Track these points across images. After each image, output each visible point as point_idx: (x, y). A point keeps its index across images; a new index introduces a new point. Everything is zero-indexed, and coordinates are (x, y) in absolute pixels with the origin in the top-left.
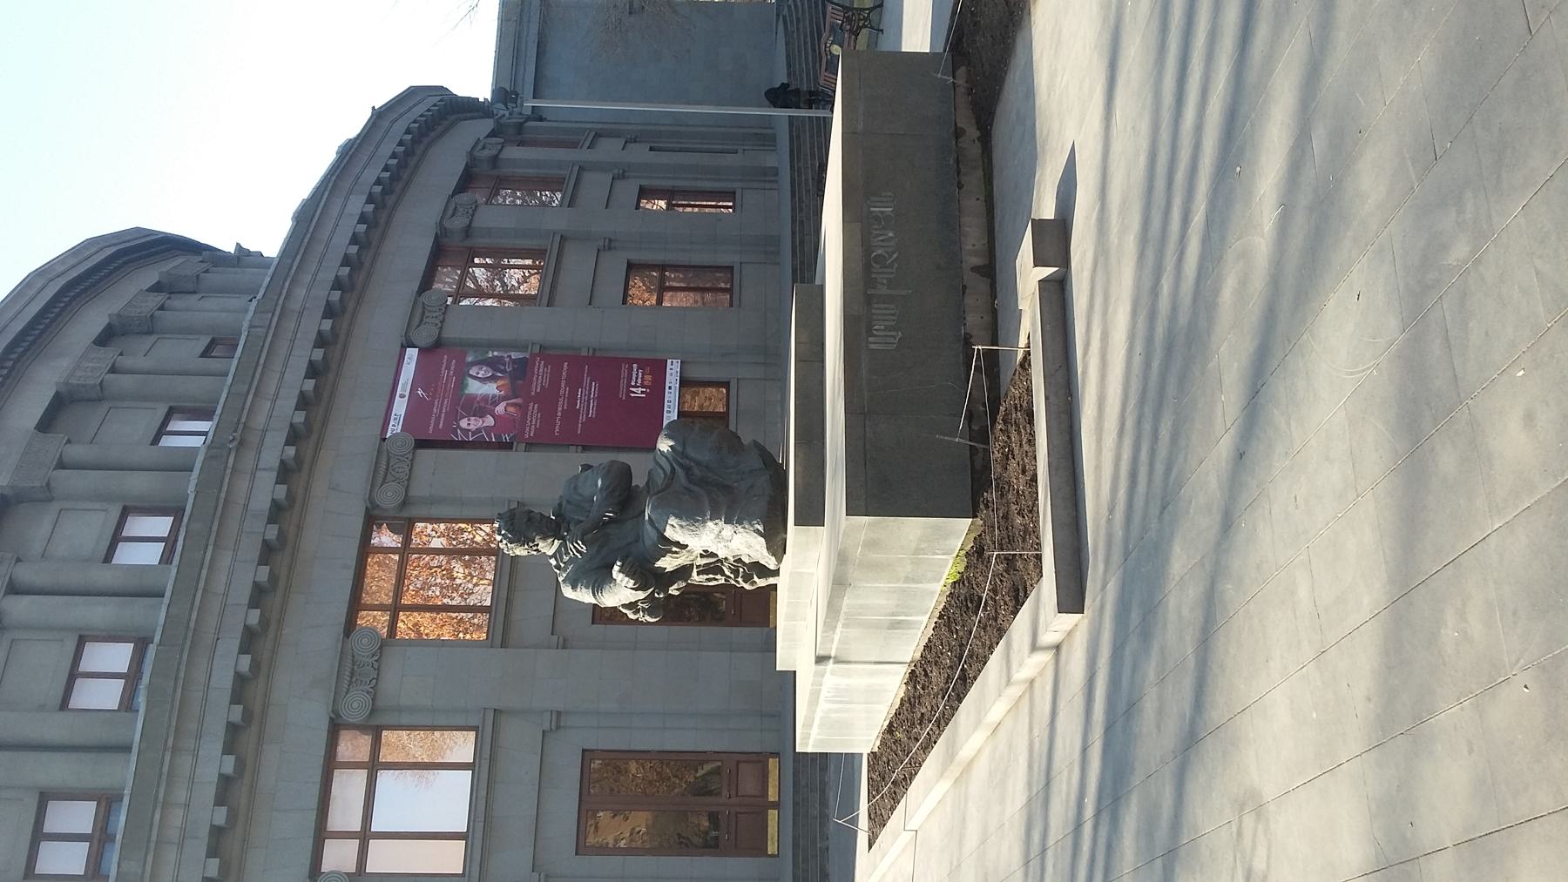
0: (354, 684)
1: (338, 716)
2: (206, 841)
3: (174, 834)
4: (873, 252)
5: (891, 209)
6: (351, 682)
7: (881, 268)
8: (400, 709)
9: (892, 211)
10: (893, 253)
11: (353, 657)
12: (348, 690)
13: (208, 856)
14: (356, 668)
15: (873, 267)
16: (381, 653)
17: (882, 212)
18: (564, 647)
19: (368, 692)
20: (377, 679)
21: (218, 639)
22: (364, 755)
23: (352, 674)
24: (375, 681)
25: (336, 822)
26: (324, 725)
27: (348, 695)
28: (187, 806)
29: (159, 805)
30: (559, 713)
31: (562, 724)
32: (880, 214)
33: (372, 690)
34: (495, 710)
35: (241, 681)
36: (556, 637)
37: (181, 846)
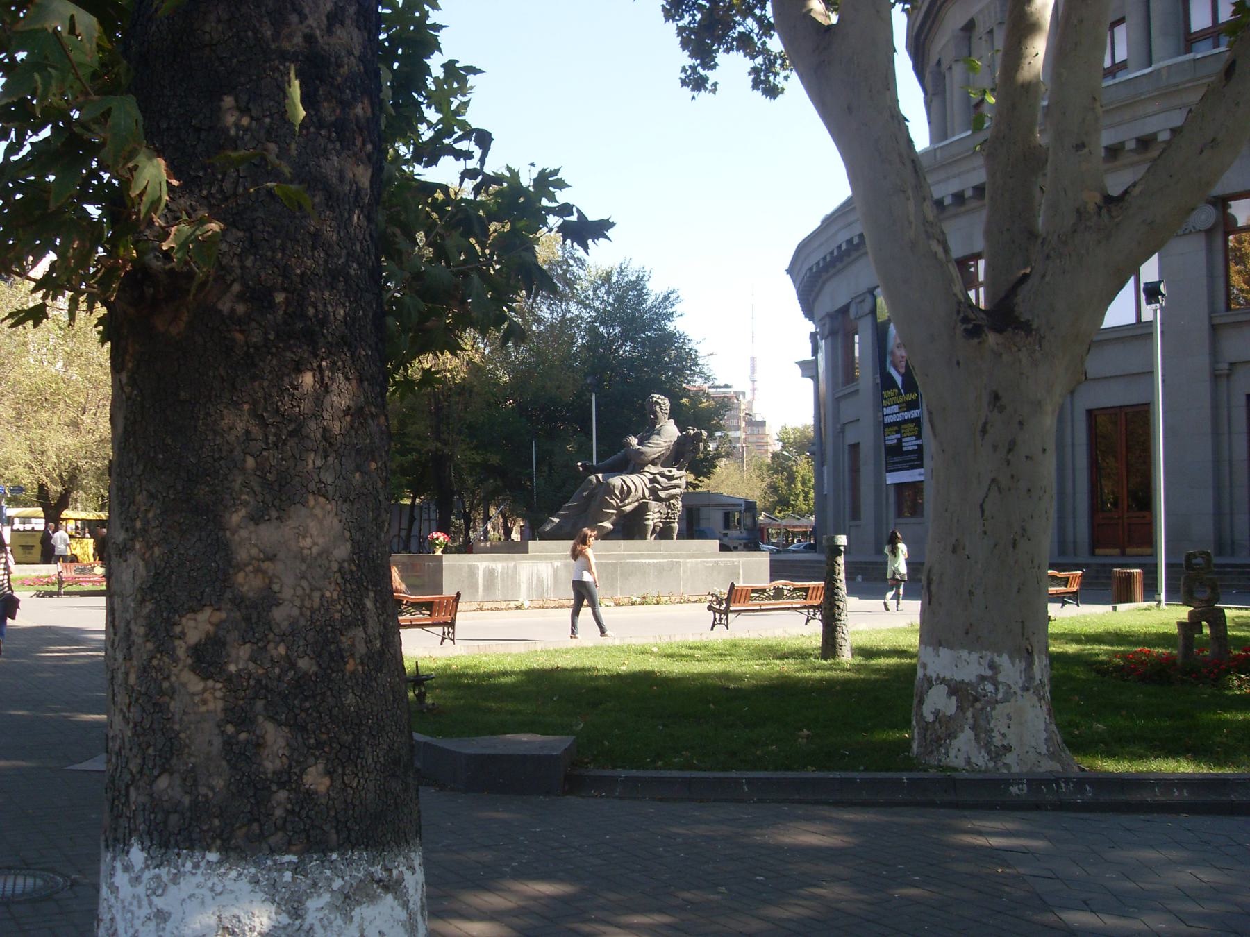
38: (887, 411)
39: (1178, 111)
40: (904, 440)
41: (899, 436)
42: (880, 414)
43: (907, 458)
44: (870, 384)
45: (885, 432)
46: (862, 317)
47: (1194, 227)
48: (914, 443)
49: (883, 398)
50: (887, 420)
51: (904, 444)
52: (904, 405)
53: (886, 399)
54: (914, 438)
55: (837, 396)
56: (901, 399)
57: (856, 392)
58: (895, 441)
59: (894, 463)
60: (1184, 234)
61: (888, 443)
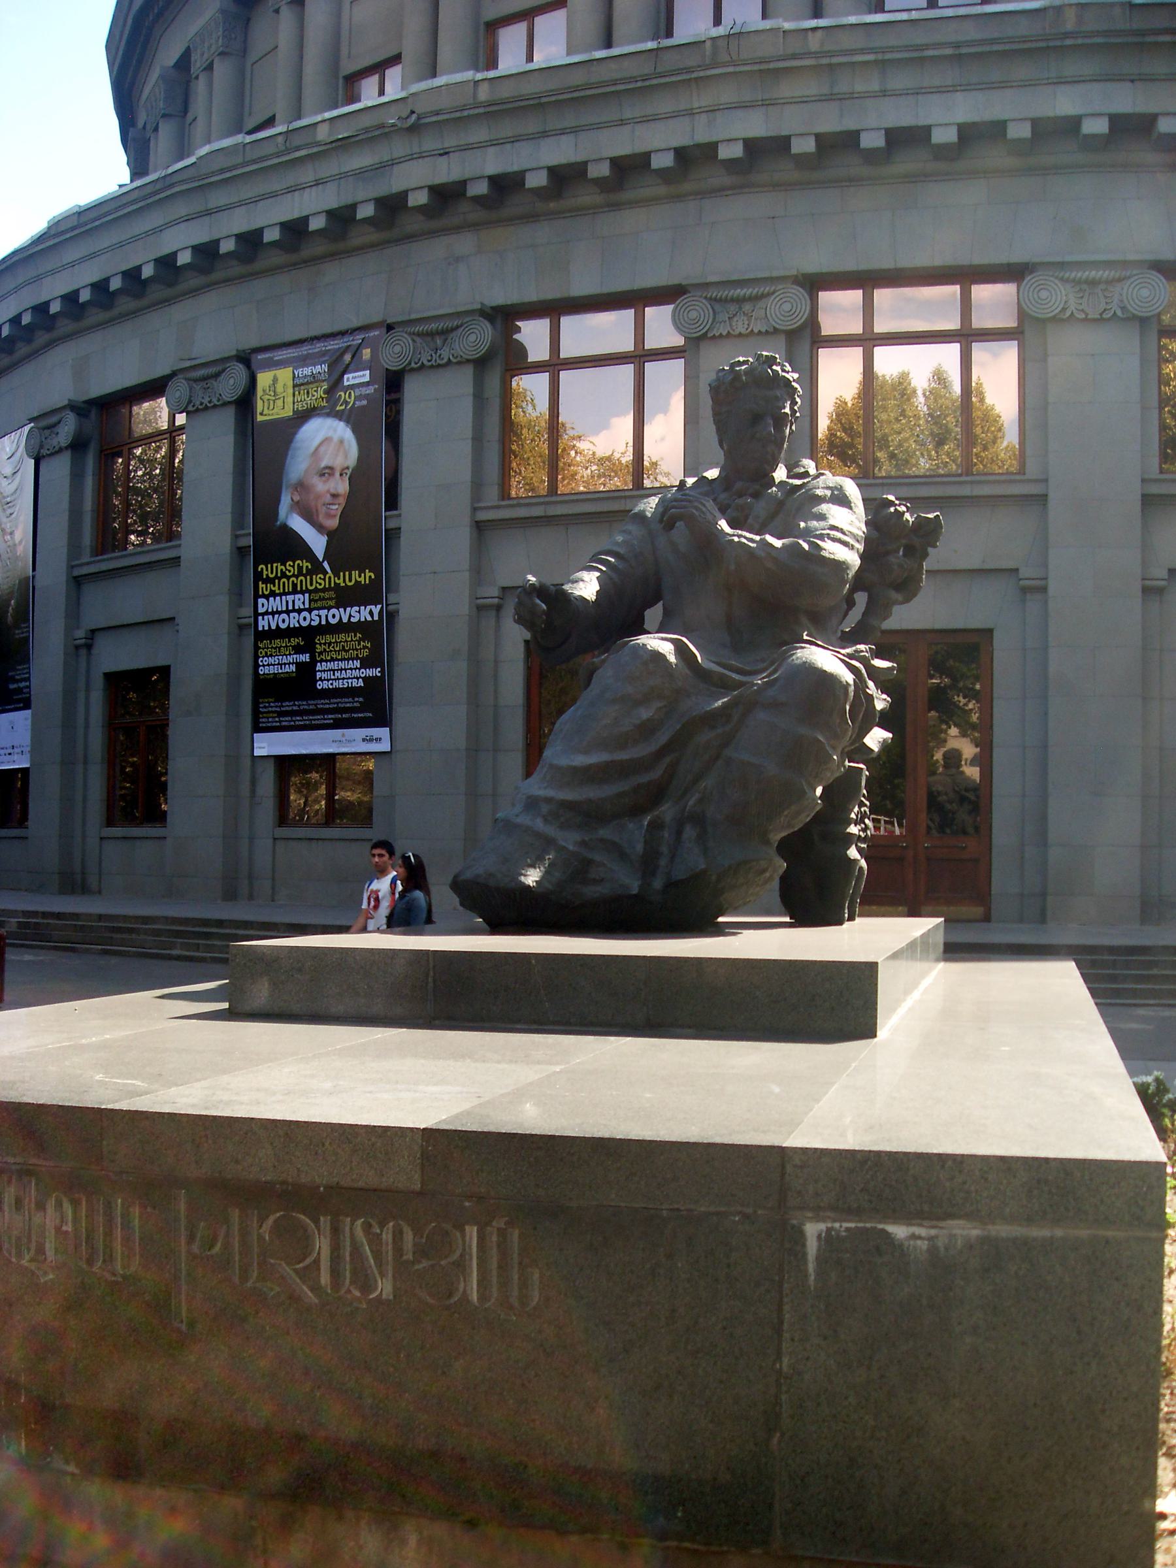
0: (1078, 288)
1: (1032, 272)
2: (838, 128)
3: (843, 87)
4: (316, 1221)
5: (474, 1297)
6: (1076, 282)
7: (261, 1238)
8: (1044, 359)
9: (465, 1297)
10: (316, 1288)
11: (1120, 280)
12: (1067, 281)
13: (819, 137)
14: (1102, 286)
15: (262, 1220)
16: (1127, 319)
17: (461, 1265)
18: (1147, 591)
19: (1064, 310)
20: (1086, 320)
21: (1132, 81)
22: (980, 321)
23: (1093, 283)
24: (1084, 316)
25: (882, 296)
26: (1017, 256)
27: (1057, 281)
28: (884, 93)
29: (880, 57)
30: (1044, 590)
31: (1028, 596)
32: (455, 1256)
33: (1068, 314)
34: (1047, 495)
35: (1072, 125)
36: (1166, 577)
37: (830, 98)
38: (263, 605)
39: (1129, 84)
40: (319, 667)
41: (305, 658)
42: (248, 611)
43: (323, 704)
44: (224, 544)
45: (257, 648)
46: (206, 408)
47: (1123, 308)
48: (356, 673)
49: (258, 576)
50: (263, 624)
51: (319, 675)
52: (332, 594)
53: (268, 581)
54: (357, 664)
55: (76, 573)
56: (319, 581)
57: (176, 561)
58: (293, 668)
59: (281, 714)
60: (1100, 320)
61: (261, 671)
